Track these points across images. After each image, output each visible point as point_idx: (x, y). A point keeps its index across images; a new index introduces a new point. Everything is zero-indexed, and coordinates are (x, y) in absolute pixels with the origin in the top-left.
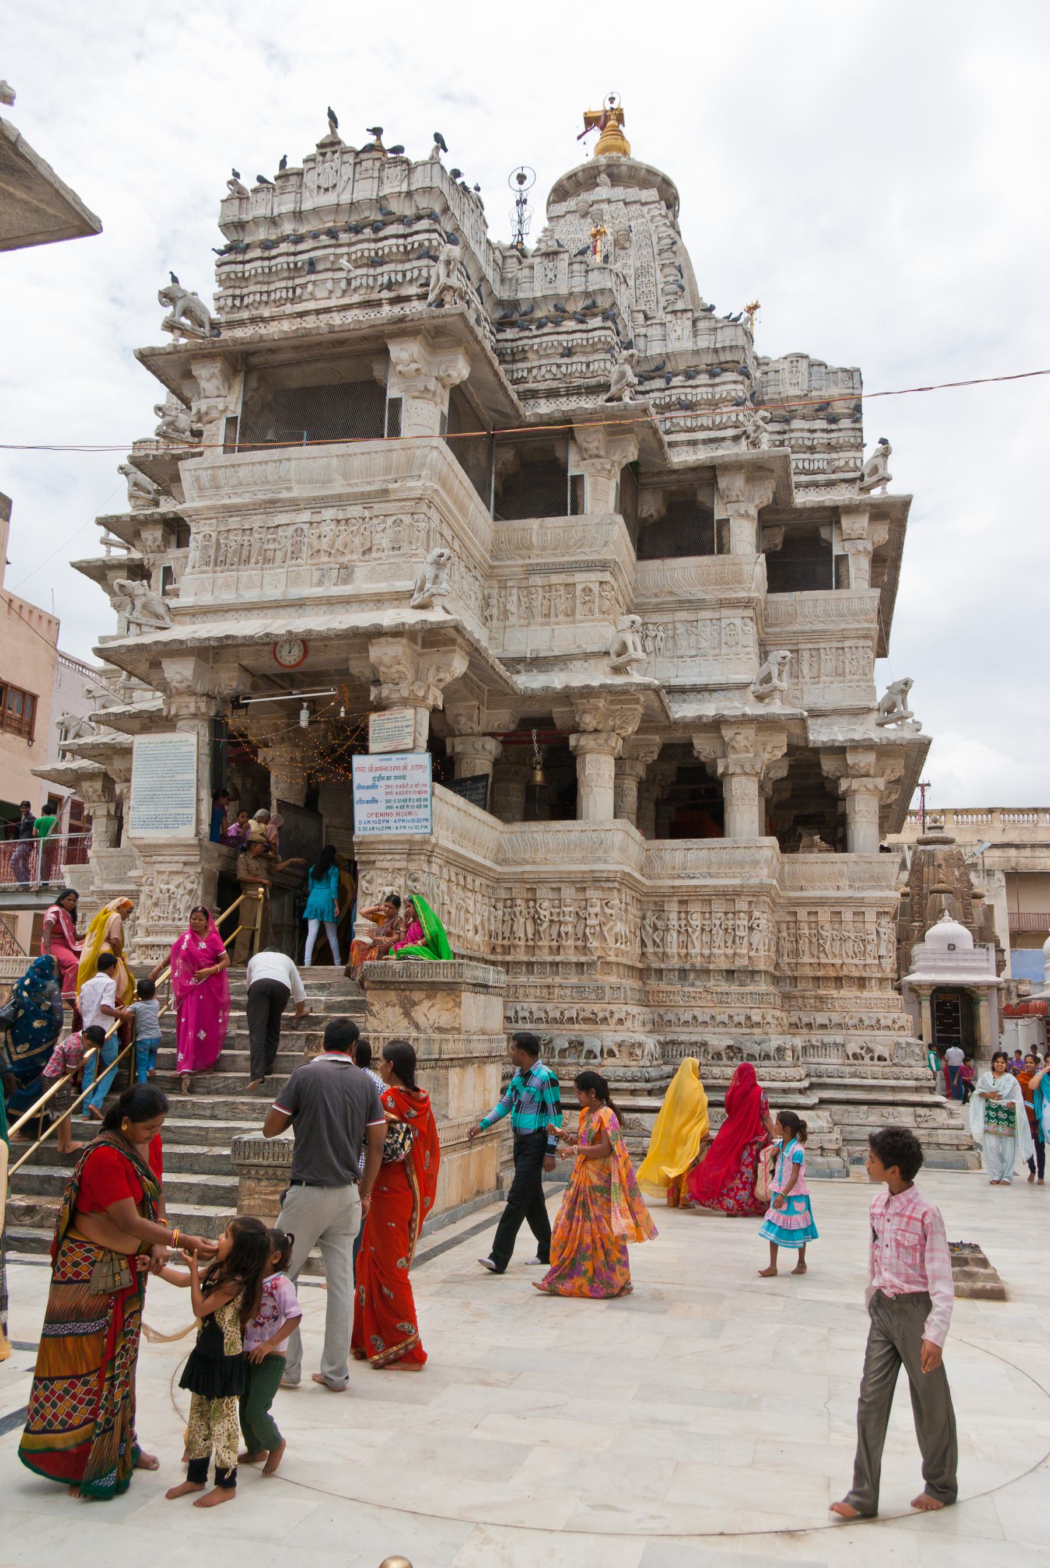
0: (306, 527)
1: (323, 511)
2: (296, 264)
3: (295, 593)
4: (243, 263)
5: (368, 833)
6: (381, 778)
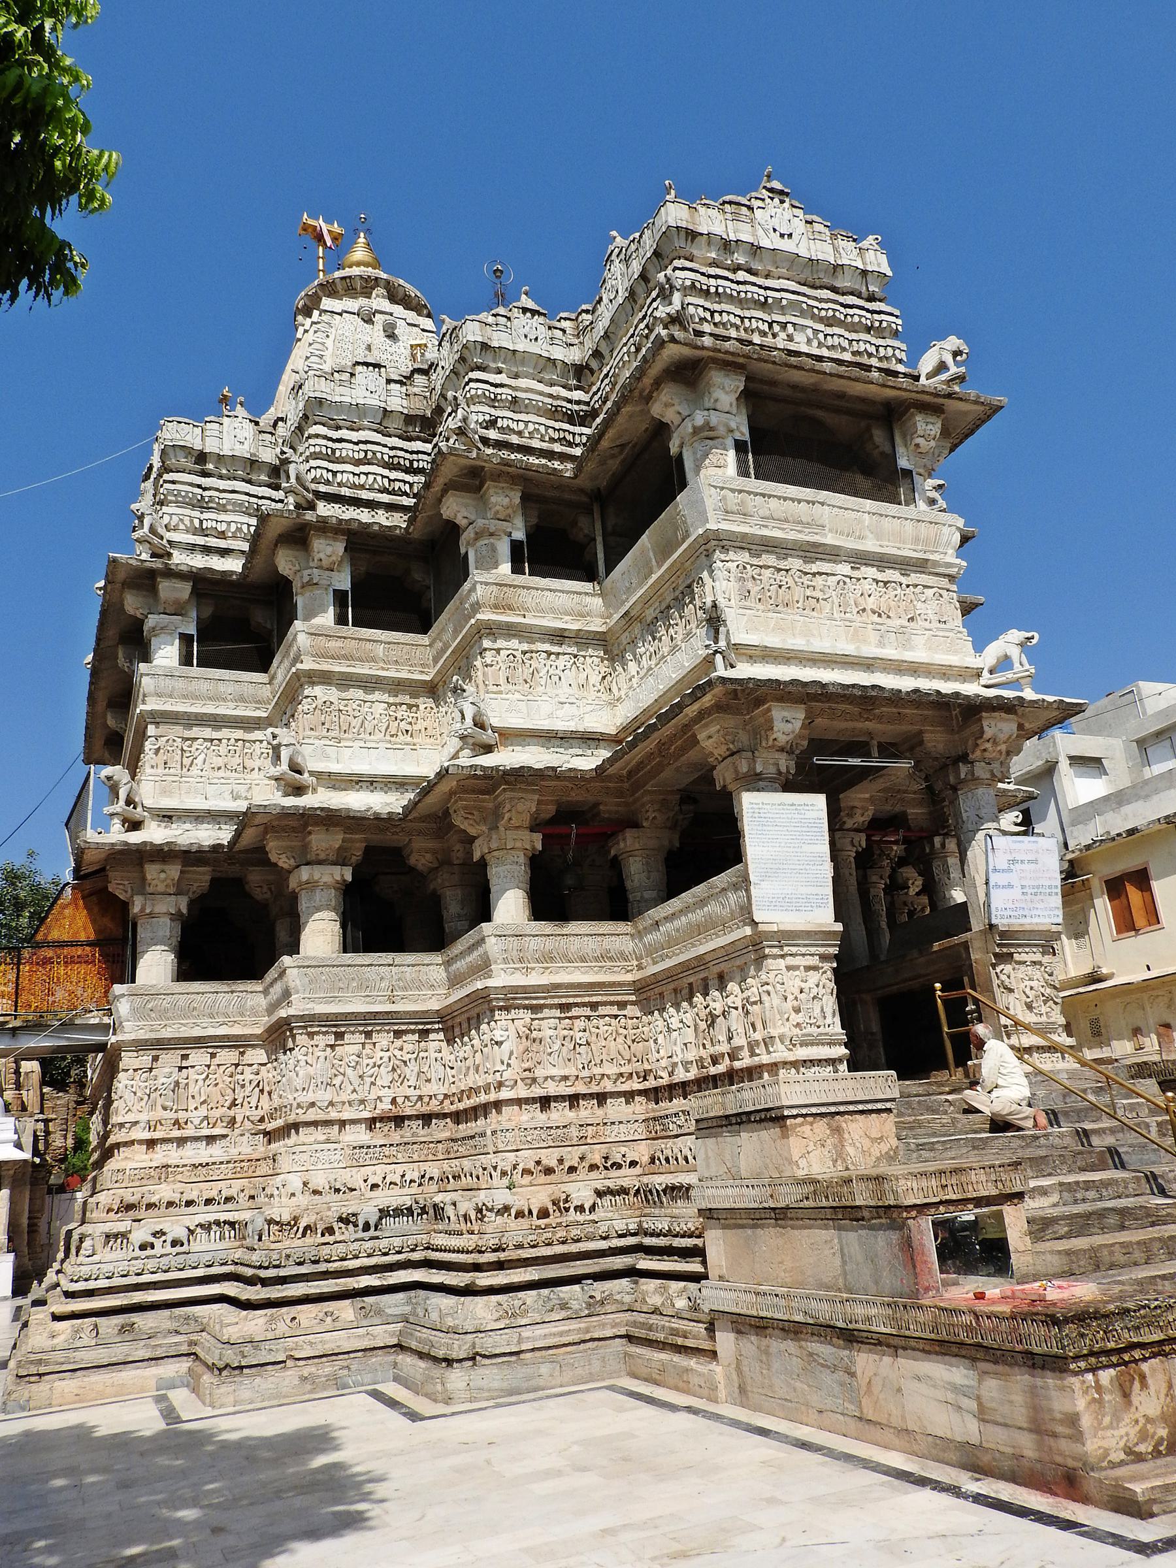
0: (847, 580)
1: (863, 568)
2: (766, 298)
3: (870, 650)
4: (709, 276)
5: (1013, 921)
6: (1014, 861)
